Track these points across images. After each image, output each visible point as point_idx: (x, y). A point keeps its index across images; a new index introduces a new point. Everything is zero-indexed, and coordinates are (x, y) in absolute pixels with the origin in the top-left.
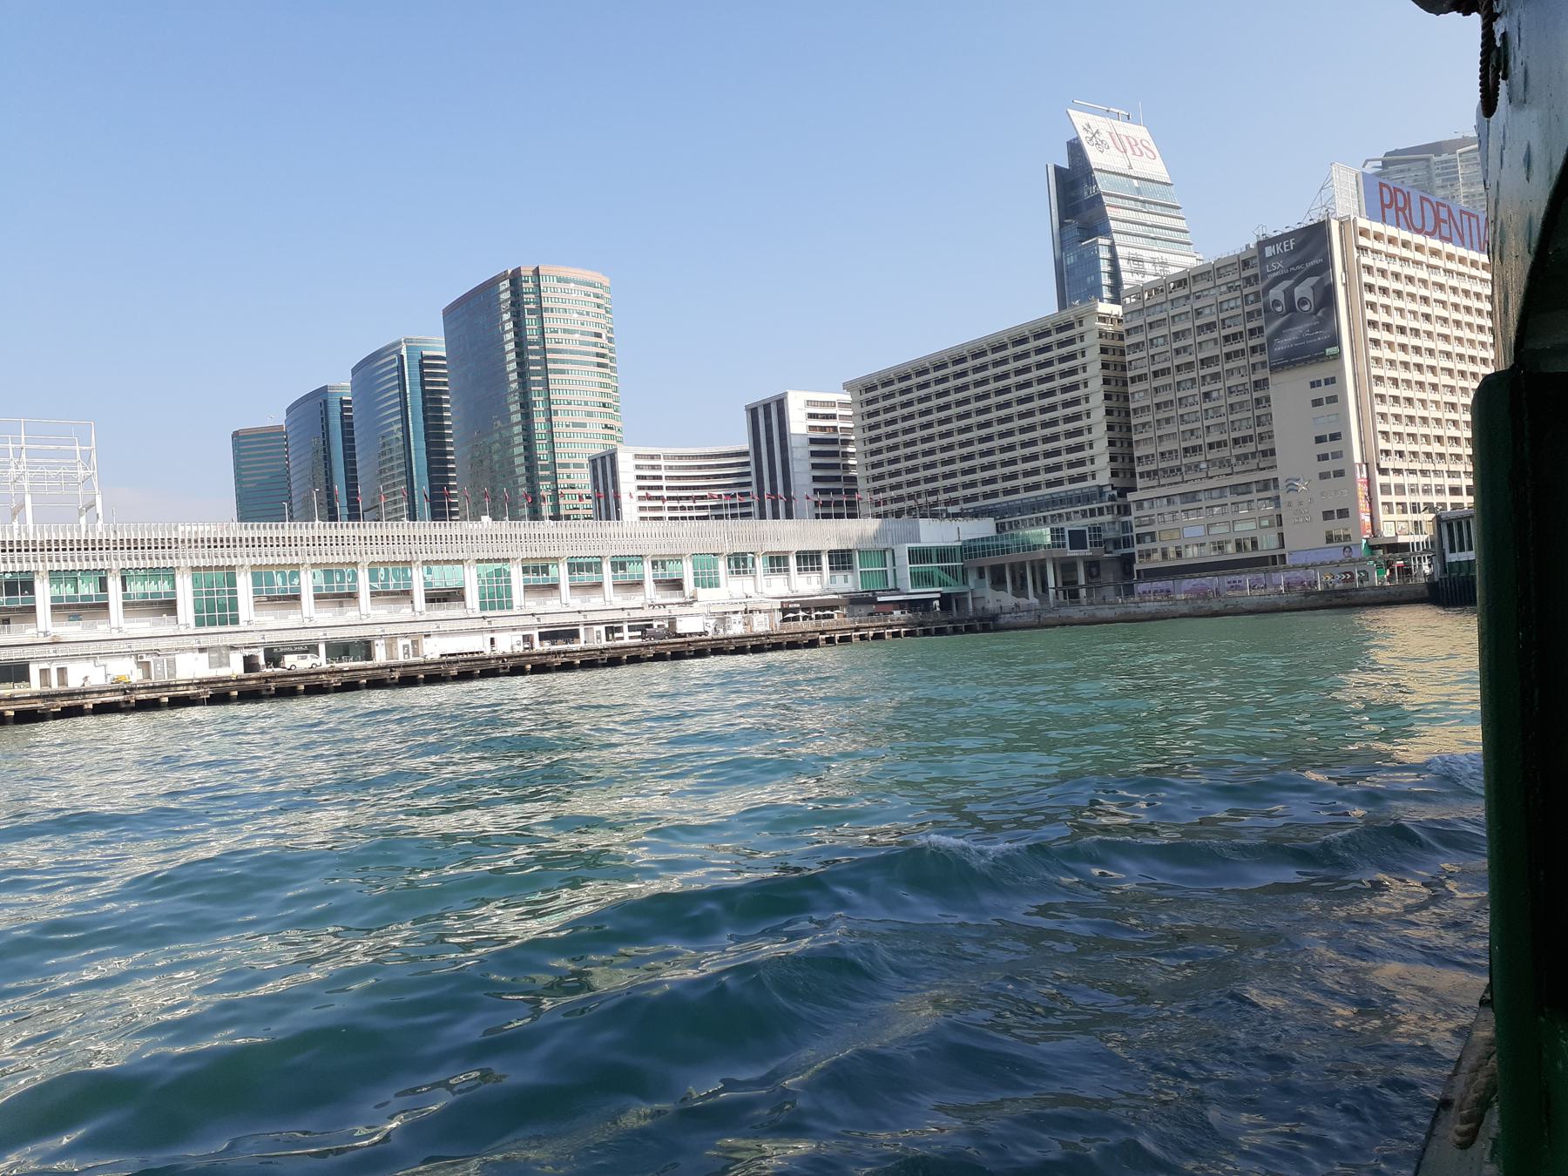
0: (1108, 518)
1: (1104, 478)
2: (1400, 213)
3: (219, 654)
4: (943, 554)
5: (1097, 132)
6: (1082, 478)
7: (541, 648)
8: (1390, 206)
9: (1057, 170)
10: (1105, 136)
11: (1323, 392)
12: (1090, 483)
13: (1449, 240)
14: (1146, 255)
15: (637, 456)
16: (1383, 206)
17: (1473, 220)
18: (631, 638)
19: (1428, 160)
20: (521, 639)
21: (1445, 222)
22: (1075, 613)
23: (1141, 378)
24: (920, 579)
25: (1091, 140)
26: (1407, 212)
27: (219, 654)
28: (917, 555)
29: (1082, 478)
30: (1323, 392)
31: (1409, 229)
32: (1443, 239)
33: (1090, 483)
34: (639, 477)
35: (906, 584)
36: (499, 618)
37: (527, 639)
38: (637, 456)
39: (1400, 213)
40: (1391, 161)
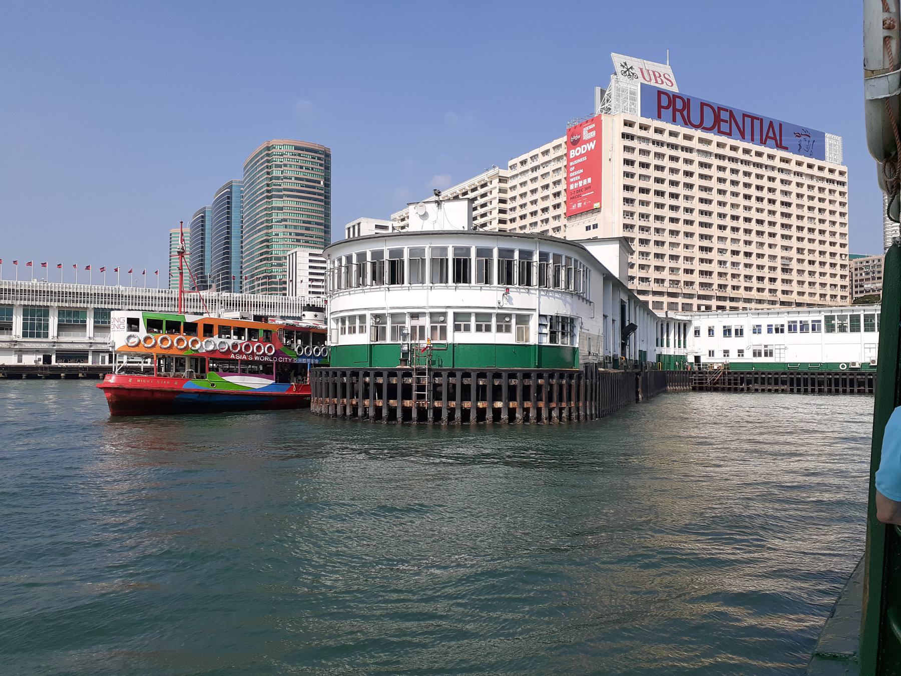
2: (678, 114)
5: (631, 68)
7: (57, 364)
8: (667, 108)
10: (636, 71)
13: (729, 134)
15: (310, 254)
16: (660, 107)
17: (757, 123)
18: (128, 362)
20: (42, 357)
21: (726, 121)
25: (625, 72)
26: (685, 113)
31: (686, 124)
32: (720, 132)
34: (310, 267)
36: (33, 343)
37: (47, 359)
38: (310, 254)
39: (678, 114)
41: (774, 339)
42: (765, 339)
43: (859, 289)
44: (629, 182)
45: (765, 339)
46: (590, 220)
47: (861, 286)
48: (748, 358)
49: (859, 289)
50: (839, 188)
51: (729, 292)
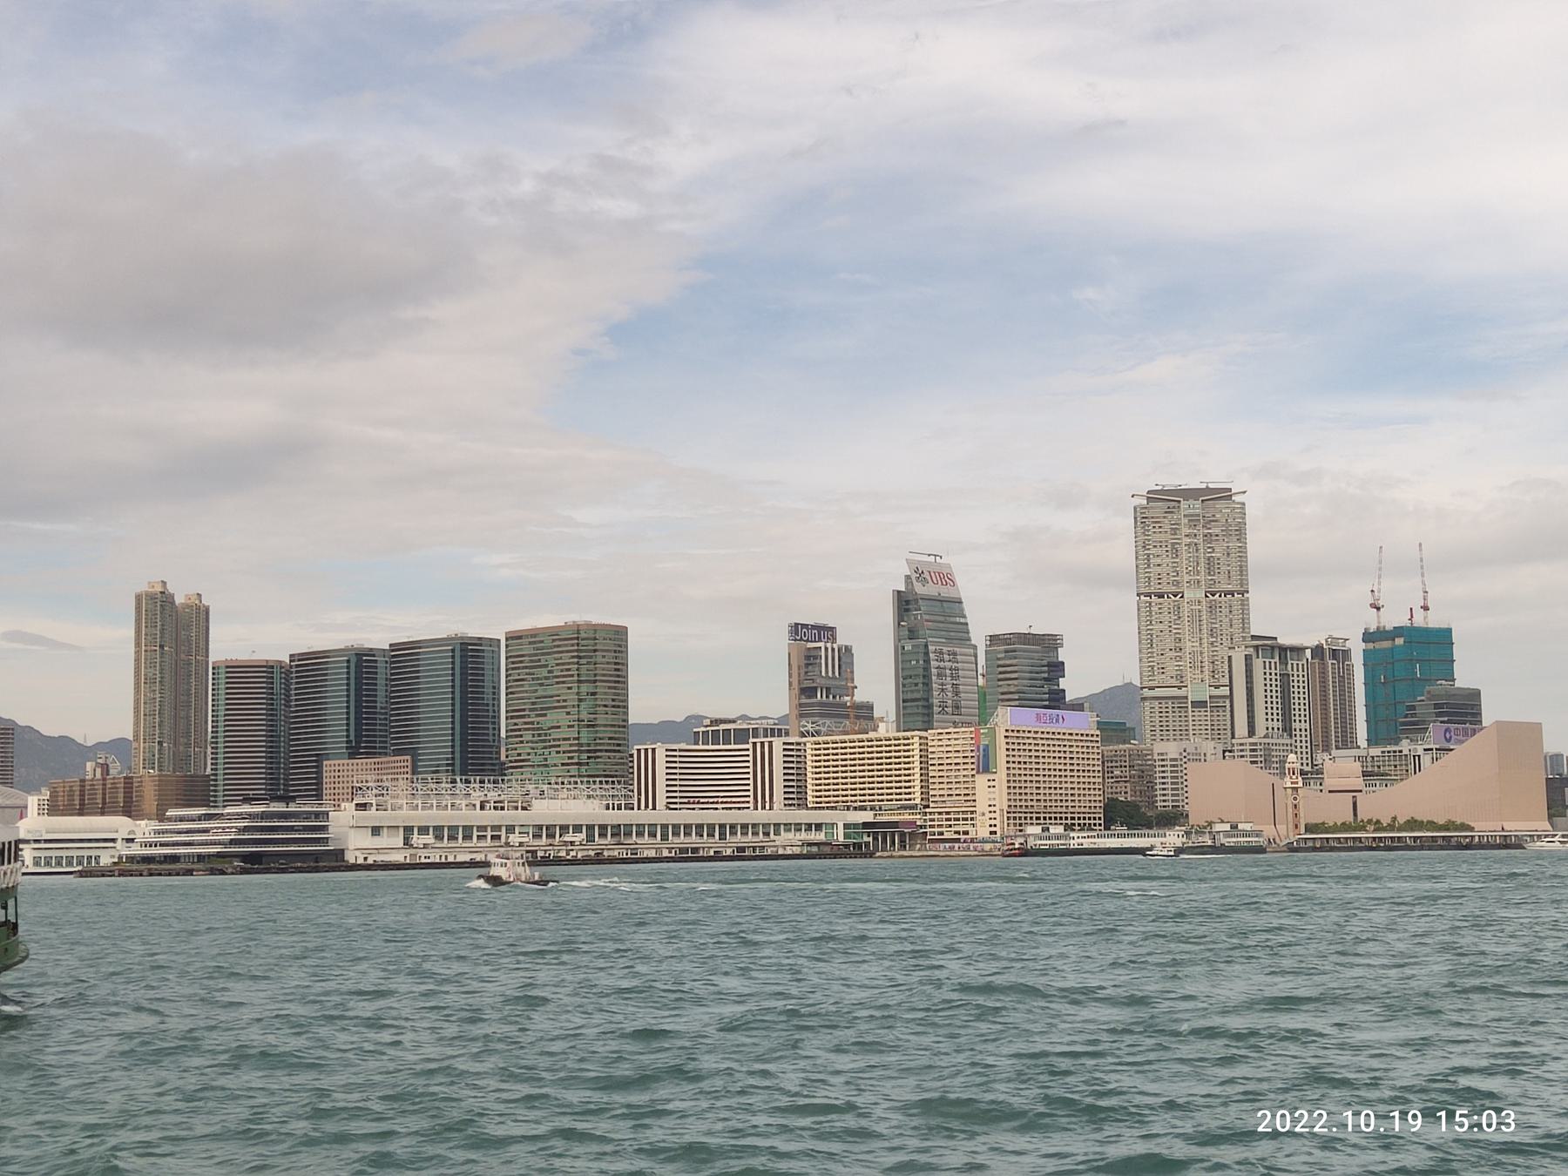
0: (918, 817)
1: (918, 801)
3: (670, 849)
4: (855, 826)
6: (910, 800)
9: (899, 592)
10: (926, 575)
11: (992, 783)
12: (912, 802)
14: (945, 649)
19: (1179, 502)
22: (905, 853)
23: (934, 765)
24: (846, 836)
27: (670, 849)
28: (846, 826)
29: (910, 800)
30: (992, 783)
33: (912, 802)
35: (841, 839)
40: (1154, 496)
41: (1083, 841)
42: (1080, 840)
43: (1110, 775)
44: (1008, 759)
45: (1080, 840)
46: (991, 777)
47: (1112, 772)
48: (1076, 846)
49: (1110, 775)
50: (1096, 745)
51: (1049, 810)
